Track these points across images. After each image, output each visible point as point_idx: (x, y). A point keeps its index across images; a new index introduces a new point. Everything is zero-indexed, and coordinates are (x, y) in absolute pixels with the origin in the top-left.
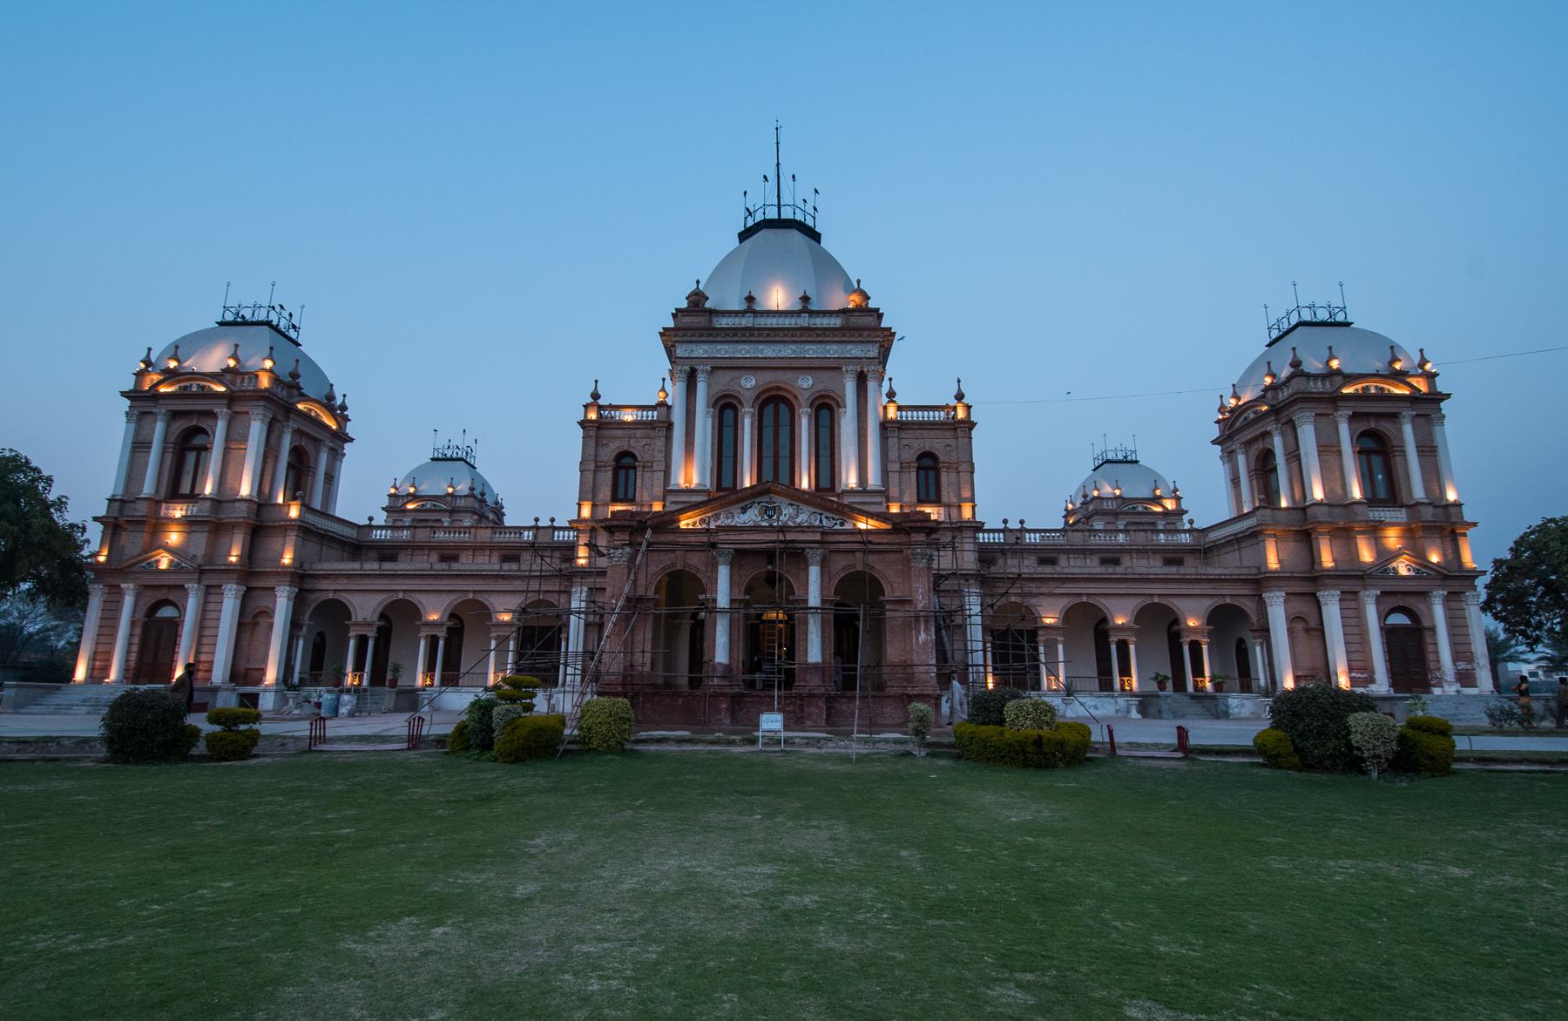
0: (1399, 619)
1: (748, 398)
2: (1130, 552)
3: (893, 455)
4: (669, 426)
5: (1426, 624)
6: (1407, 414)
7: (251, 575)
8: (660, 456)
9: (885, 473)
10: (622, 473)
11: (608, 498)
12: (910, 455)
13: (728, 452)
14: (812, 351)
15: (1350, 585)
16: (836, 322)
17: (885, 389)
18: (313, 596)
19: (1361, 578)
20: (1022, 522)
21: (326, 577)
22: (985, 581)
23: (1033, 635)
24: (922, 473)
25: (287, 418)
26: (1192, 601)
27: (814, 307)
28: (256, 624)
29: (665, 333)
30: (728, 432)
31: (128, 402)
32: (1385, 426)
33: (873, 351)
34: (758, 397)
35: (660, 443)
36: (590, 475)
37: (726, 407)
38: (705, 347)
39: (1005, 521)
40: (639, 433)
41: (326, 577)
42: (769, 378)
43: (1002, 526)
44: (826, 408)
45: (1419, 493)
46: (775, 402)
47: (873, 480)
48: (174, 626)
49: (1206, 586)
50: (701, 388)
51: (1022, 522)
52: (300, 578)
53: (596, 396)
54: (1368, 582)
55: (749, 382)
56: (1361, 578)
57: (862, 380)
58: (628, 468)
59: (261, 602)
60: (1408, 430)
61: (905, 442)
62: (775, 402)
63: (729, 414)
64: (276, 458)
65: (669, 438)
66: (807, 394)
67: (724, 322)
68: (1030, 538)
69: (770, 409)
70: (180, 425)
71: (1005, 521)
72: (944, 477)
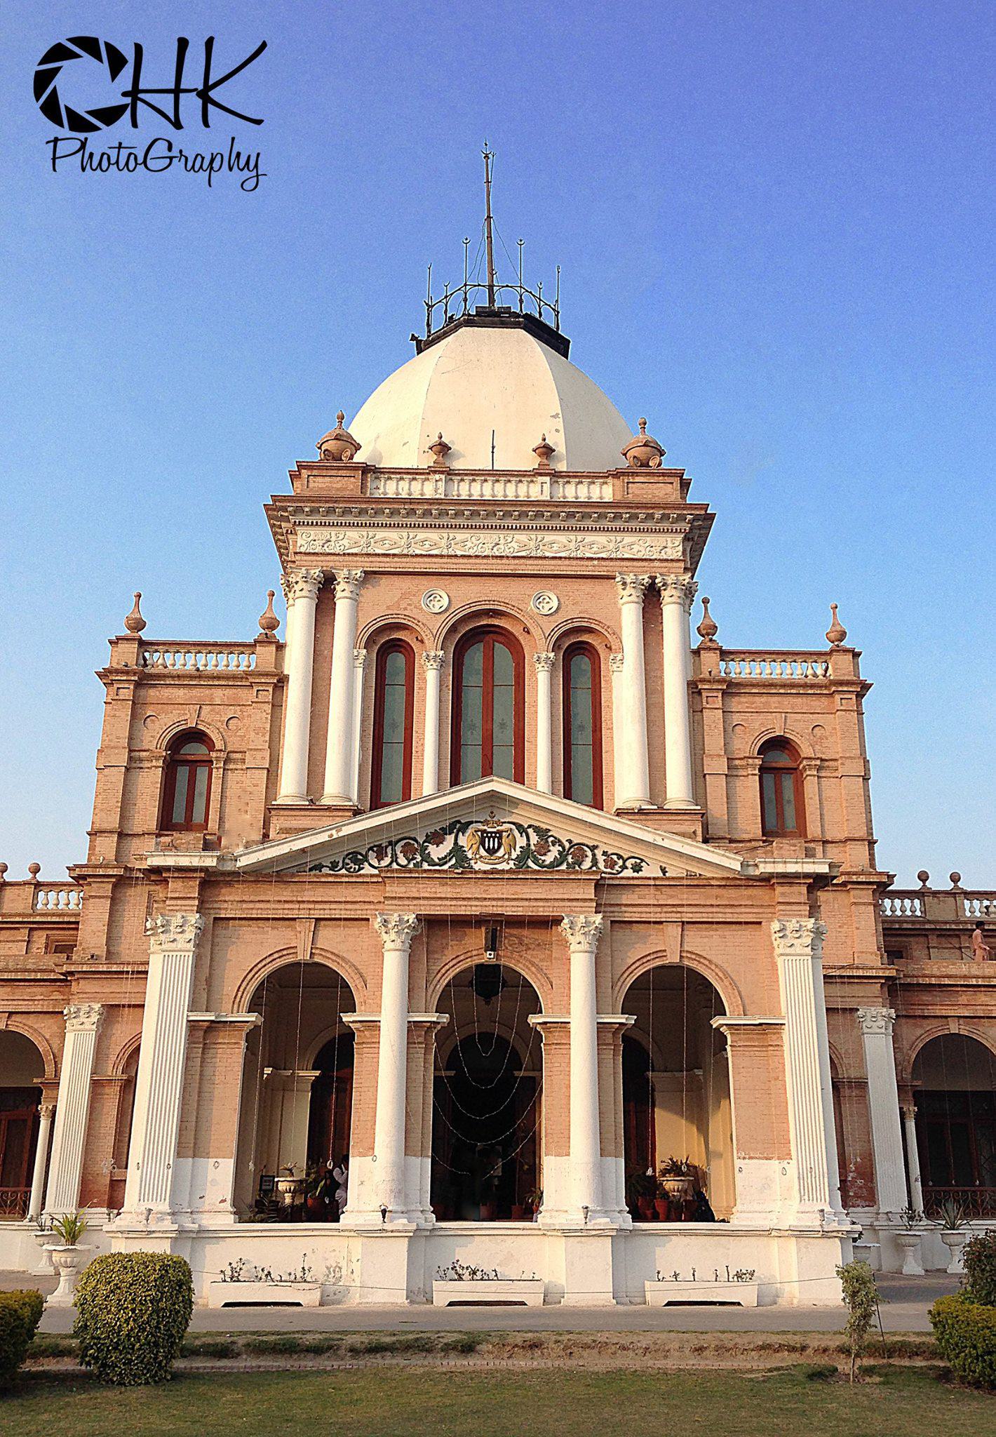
3: (714, 741)
4: (281, 682)
8: (262, 742)
9: (698, 777)
10: (183, 773)
11: (153, 825)
12: (746, 744)
13: (395, 736)
14: (559, 543)
17: (697, 620)
20: (955, 878)
24: (769, 778)
30: (395, 697)
33: (673, 546)
34: (453, 629)
35: (261, 716)
36: (118, 776)
37: (388, 648)
39: (923, 877)
40: (219, 695)
43: (917, 885)
50: (343, 607)
51: (955, 878)
57: (651, 596)
58: (194, 764)
61: (736, 719)
63: (398, 660)
65: (277, 706)
66: (549, 626)
68: (973, 909)
69: (475, 657)
71: (923, 877)
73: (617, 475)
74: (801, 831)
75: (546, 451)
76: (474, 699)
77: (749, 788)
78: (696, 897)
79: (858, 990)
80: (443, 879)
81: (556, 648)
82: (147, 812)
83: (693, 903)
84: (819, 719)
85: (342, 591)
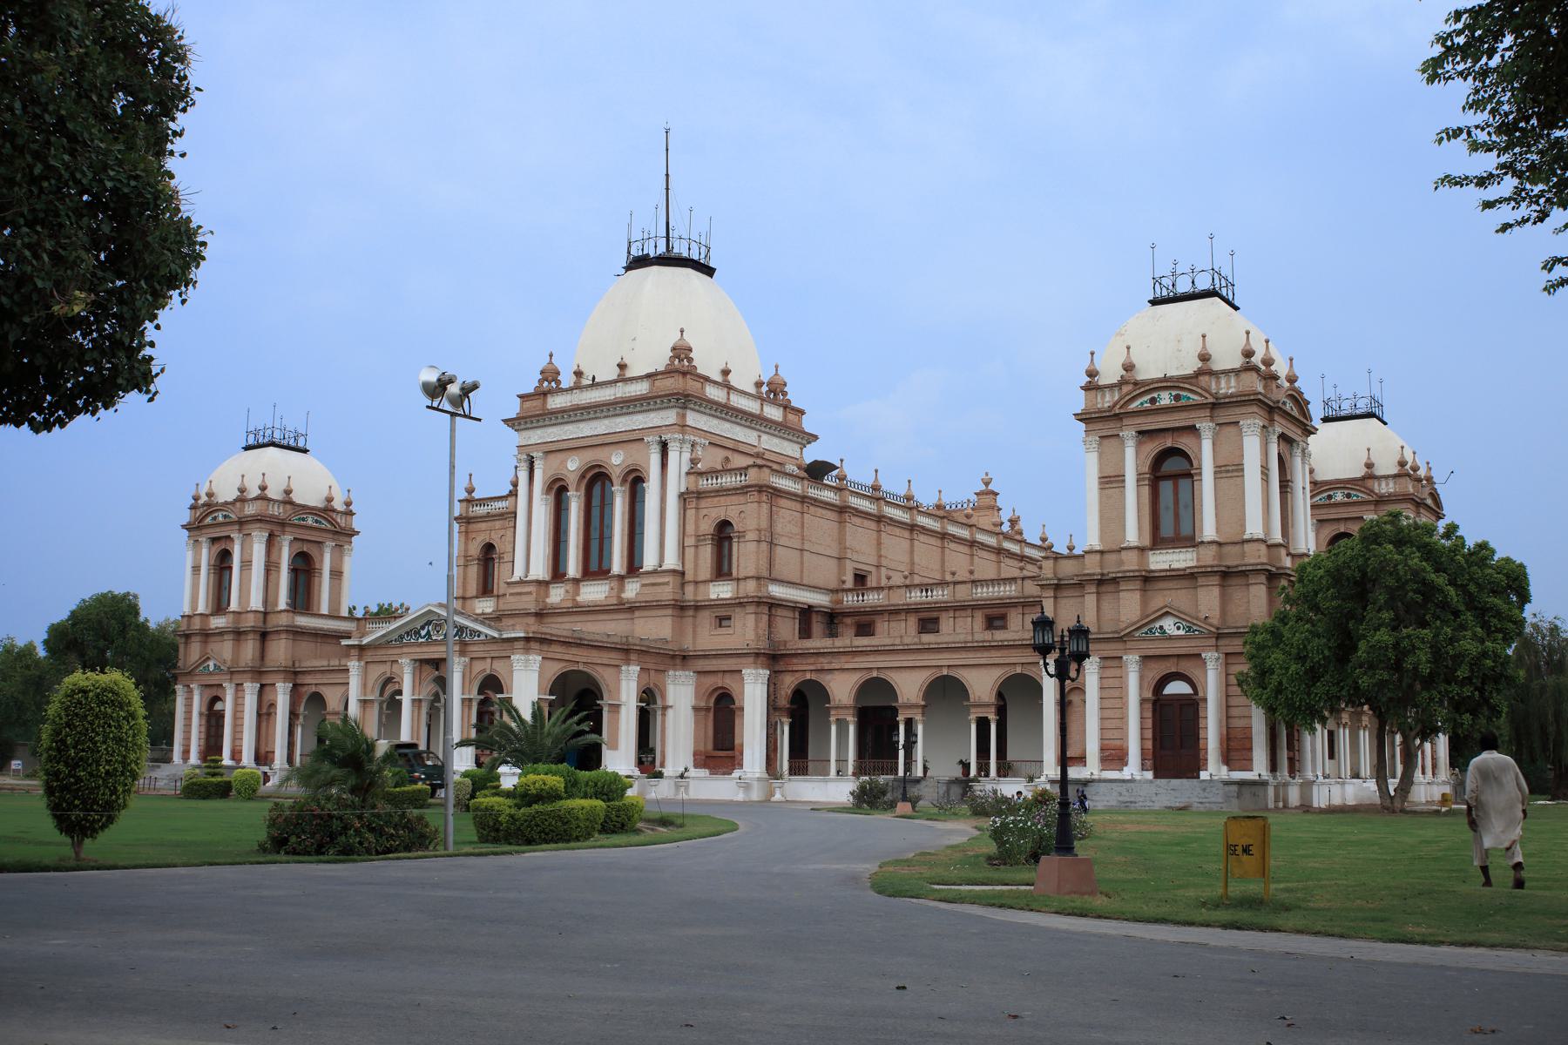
0: (1176, 688)
1: (572, 480)
2: (1014, 605)
3: (690, 529)
5: (1201, 694)
6: (1206, 427)
7: (258, 673)
9: (682, 548)
12: (708, 527)
14: (623, 424)
15: (1111, 649)
16: (641, 388)
18: (304, 689)
19: (1120, 639)
21: (309, 672)
22: (774, 659)
23: (894, 711)
25: (284, 533)
26: (983, 672)
27: (629, 374)
28: (269, 714)
29: (505, 421)
31: (186, 533)
32: (1184, 442)
34: (583, 476)
35: (509, 533)
37: (558, 490)
38: (539, 432)
40: (498, 524)
41: (309, 672)
42: (590, 457)
44: (636, 481)
45: (1209, 531)
46: (596, 479)
47: (671, 561)
48: (220, 716)
49: (994, 653)
50: (538, 474)
52: (293, 674)
53: (470, 491)
54: (1129, 645)
55: (573, 464)
56: (1120, 639)
57: (664, 447)
59: (267, 697)
60: (1207, 446)
61: (705, 512)
62: (596, 479)
64: (278, 566)
66: (618, 471)
67: (556, 402)
69: (597, 490)
70: (218, 548)
72: (735, 546)
73: (649, 376)
74: (730, 574)
75: (622, 367)
76: (596, 512)
77: (707, 552)
78: (494, 647)
79: (743, 660)
80: (427, 644)
81: (624, 481)
82: (473, 588)
83: (495, 650)
84: (742, 508)
85: (538, 465)
